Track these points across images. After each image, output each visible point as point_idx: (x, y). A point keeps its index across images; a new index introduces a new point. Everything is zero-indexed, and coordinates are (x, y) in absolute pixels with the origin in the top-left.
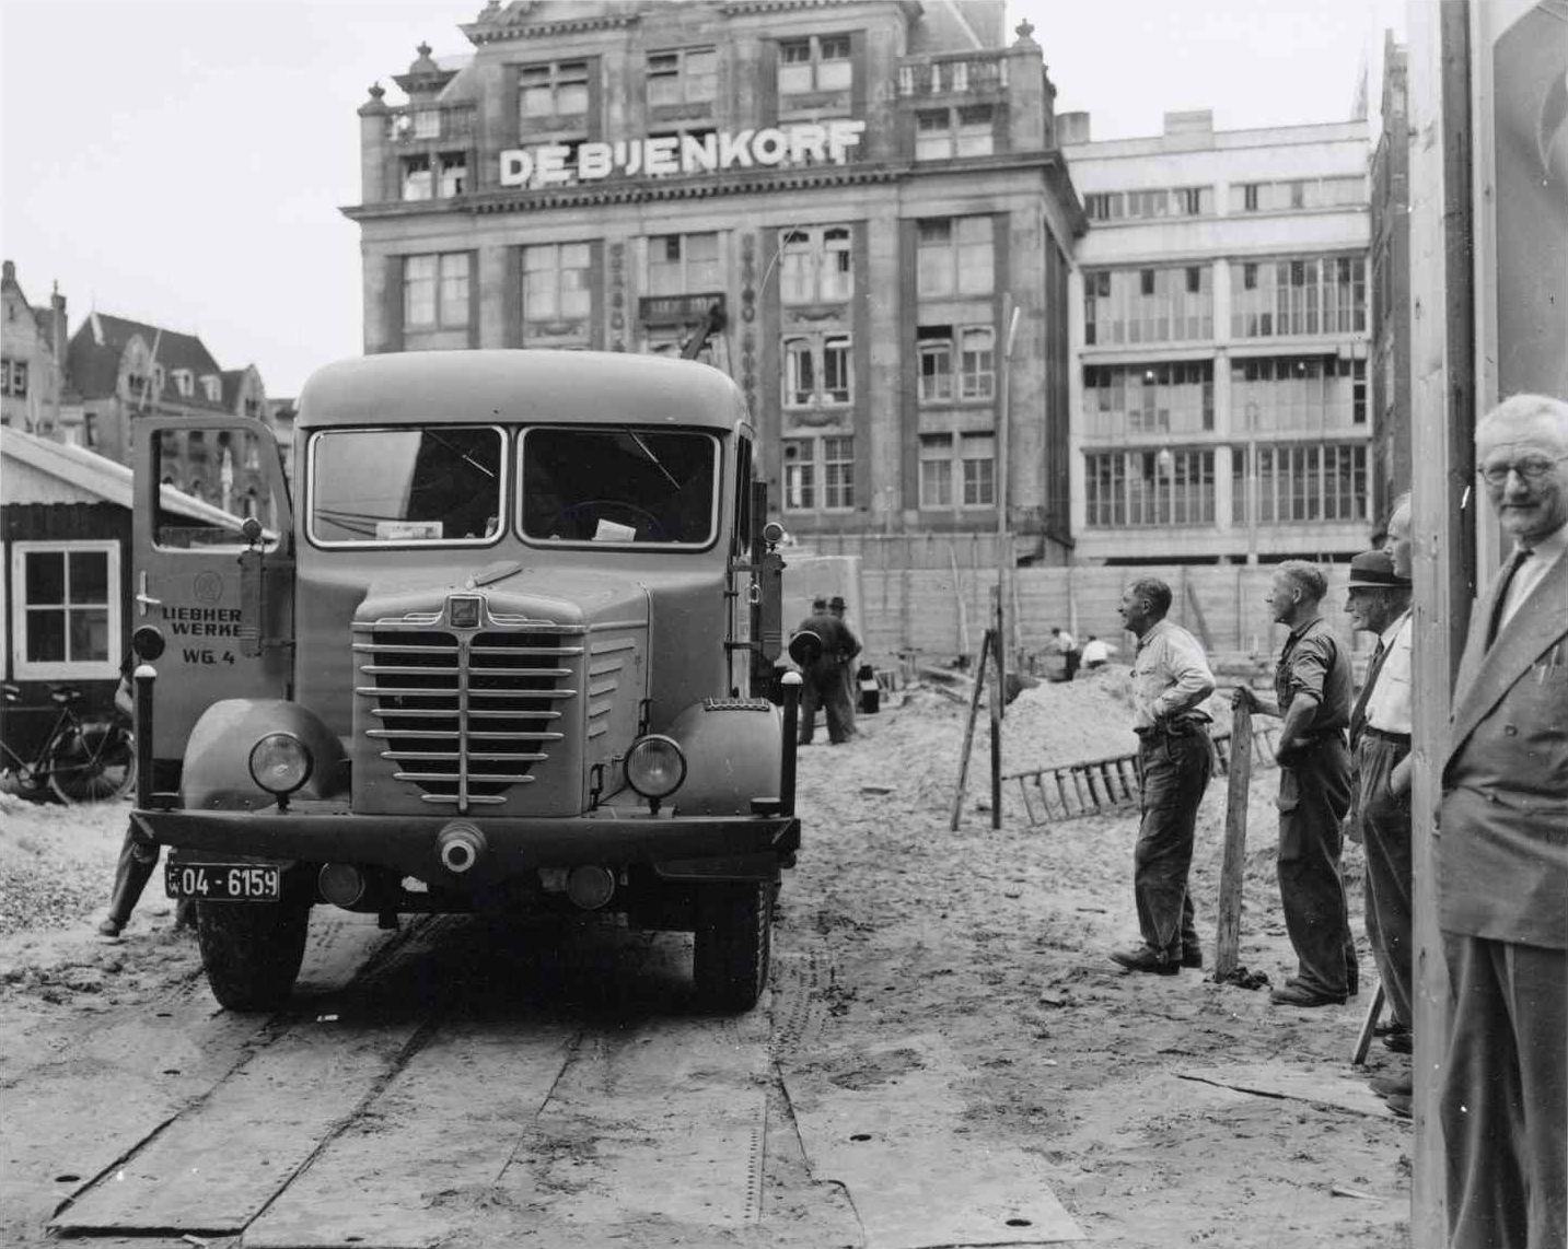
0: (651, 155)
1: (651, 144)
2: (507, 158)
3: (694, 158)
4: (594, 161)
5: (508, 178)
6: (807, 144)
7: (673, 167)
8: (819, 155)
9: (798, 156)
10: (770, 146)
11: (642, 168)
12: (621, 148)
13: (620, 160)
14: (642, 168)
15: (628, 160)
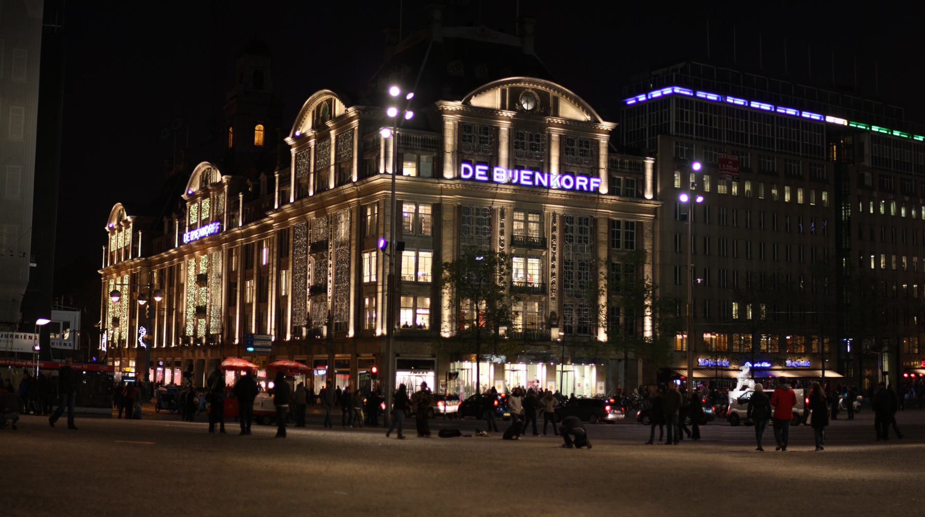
0: (523, 177)
1: (523, 172)
2: (464, 166)
3: (540, 182)
4: (498, 174)
5: (463, 176)
6: (582, 183)
7: (530, 183)
8: (585, 188)
9: (578, 187)
10: (568, 182)
11: (519, 180)
12: (510, 172)
13: (510, 175)
14: (519, 180)
15: (513, 178)
